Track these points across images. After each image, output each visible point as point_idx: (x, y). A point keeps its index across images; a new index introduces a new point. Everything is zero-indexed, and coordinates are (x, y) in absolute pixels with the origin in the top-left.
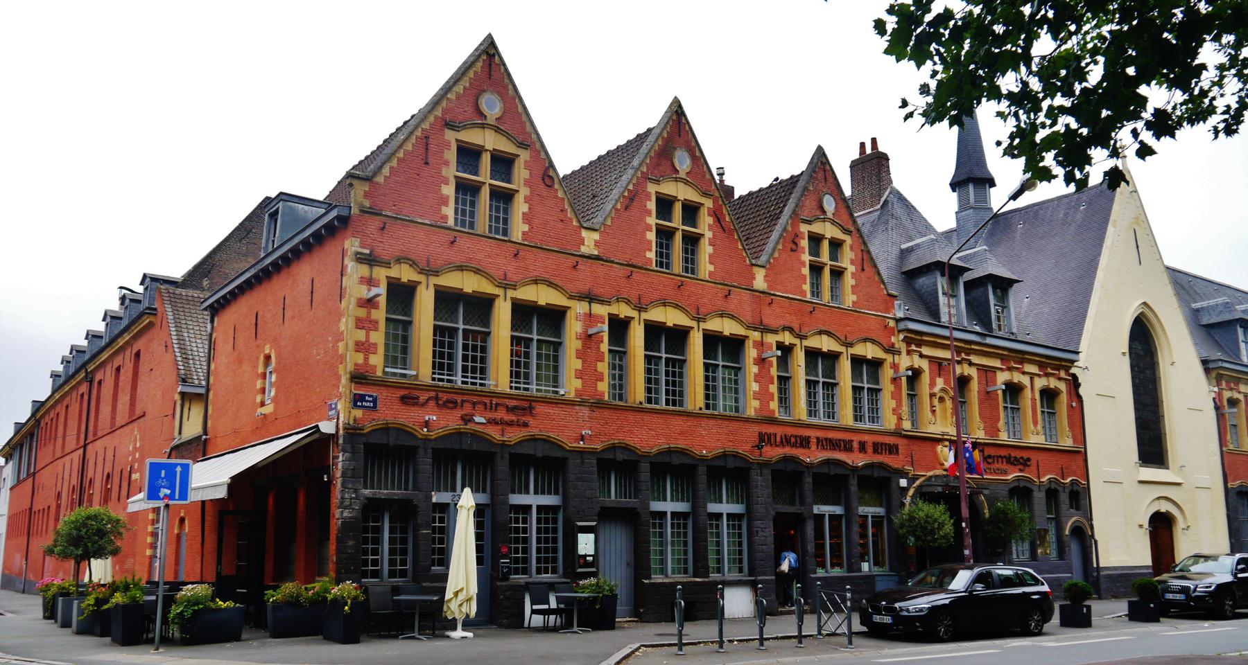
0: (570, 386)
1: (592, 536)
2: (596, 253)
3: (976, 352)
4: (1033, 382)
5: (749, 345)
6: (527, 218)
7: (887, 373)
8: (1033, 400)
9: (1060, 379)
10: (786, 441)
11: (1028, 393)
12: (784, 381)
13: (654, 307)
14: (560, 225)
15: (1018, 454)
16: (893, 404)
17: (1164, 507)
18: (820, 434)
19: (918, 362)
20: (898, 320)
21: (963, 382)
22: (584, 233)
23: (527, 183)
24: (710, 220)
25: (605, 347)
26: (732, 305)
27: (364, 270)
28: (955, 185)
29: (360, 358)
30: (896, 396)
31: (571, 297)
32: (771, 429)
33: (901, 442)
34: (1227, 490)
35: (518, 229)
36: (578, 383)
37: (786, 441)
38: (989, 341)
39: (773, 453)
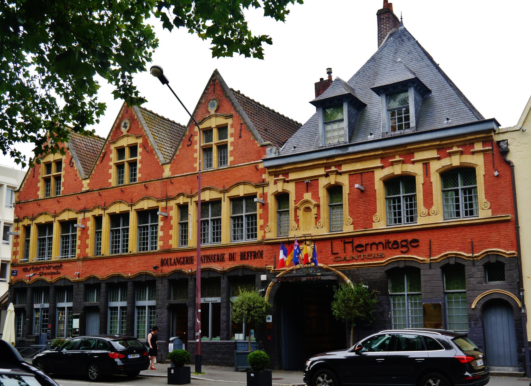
1: (78, 320)
2: (88, 189)
3: (345, 162)
10: (178, 261)
13: (153, 200)
14: (75, 182)
15: (399, 238)
18: (243, 250)
22: (84, 182)
26: (150, 192)
31: (77, 213)
32: (168, 256)
33: (265, 248)
37: (178, 261)
39: (168, 270)
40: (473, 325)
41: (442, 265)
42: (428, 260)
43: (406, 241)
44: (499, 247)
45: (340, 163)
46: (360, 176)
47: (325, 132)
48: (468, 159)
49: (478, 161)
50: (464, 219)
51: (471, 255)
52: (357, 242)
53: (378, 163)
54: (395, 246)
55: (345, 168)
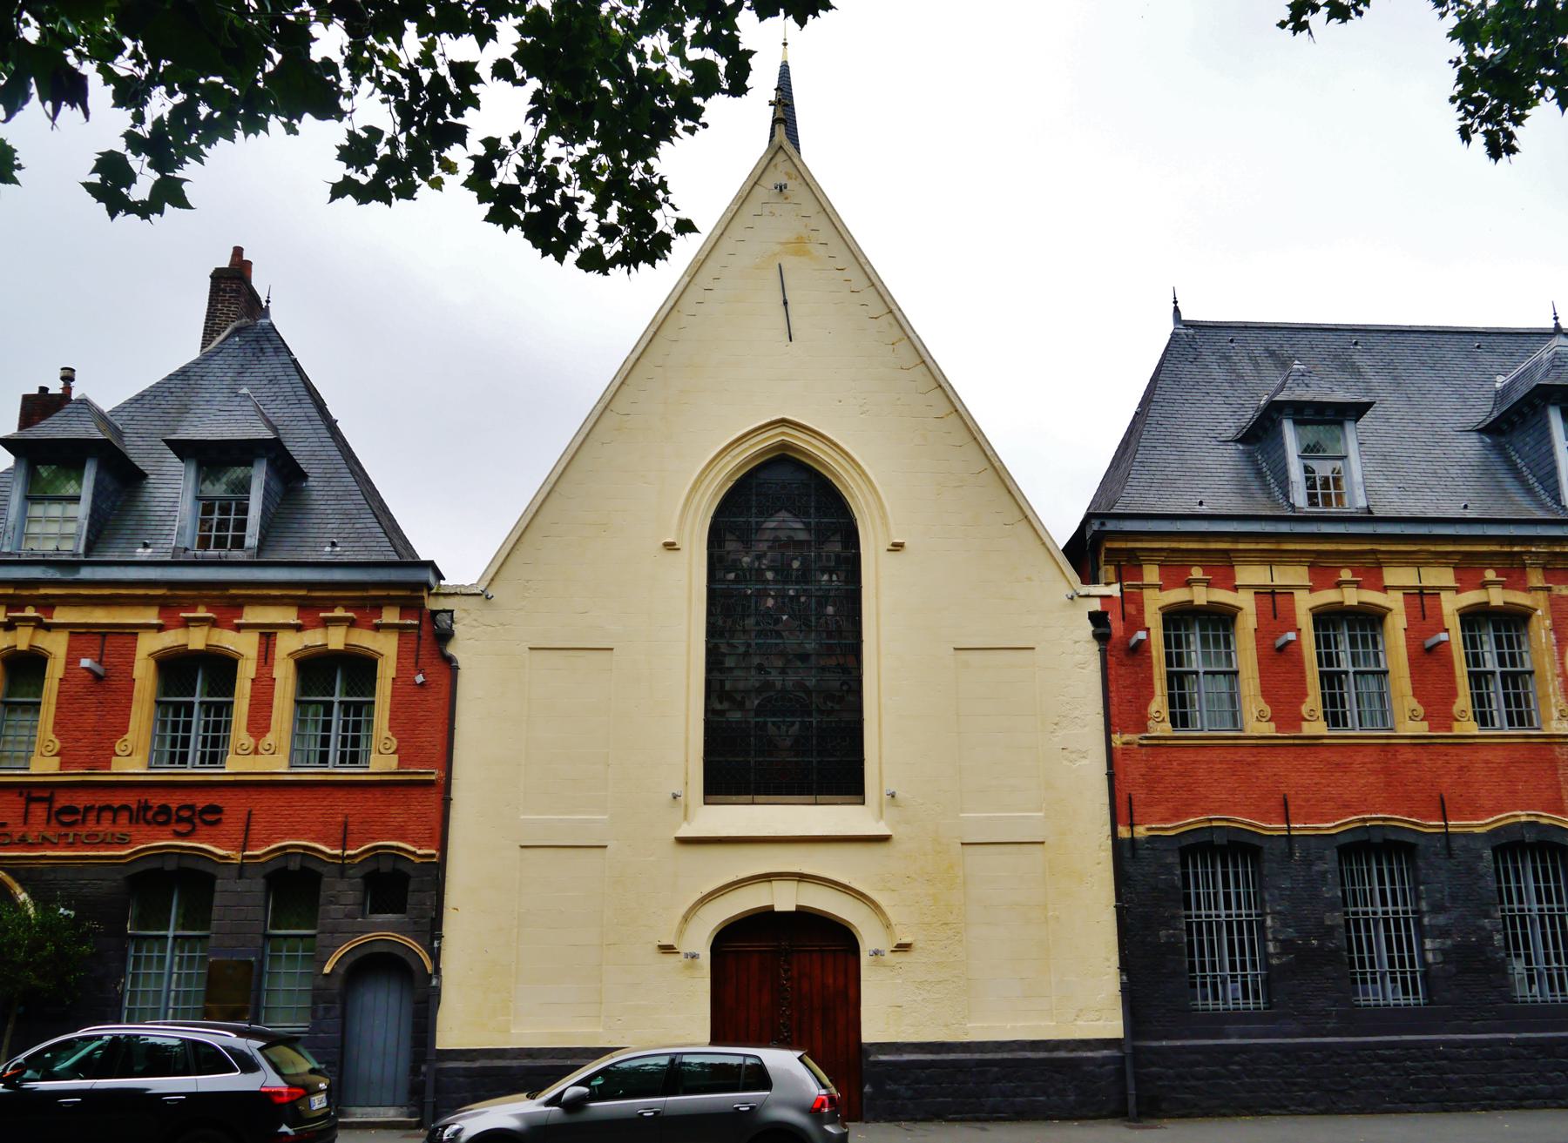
3: (66, 601)
15: (174, 801)
40: (320, 1014)
41: (269, 869)
42: (236, 857)
43: (191, 807)
44: (402, 838)
45: (51, 601)
46: (98, 641)
47: (25, 518)
48: (365, 640)
49: (386, 647)
50: (336, 770)
51: (338, 852)
52: (62, 800)
53: (151, 616)
54: (161, 819)
55: (61, 616)
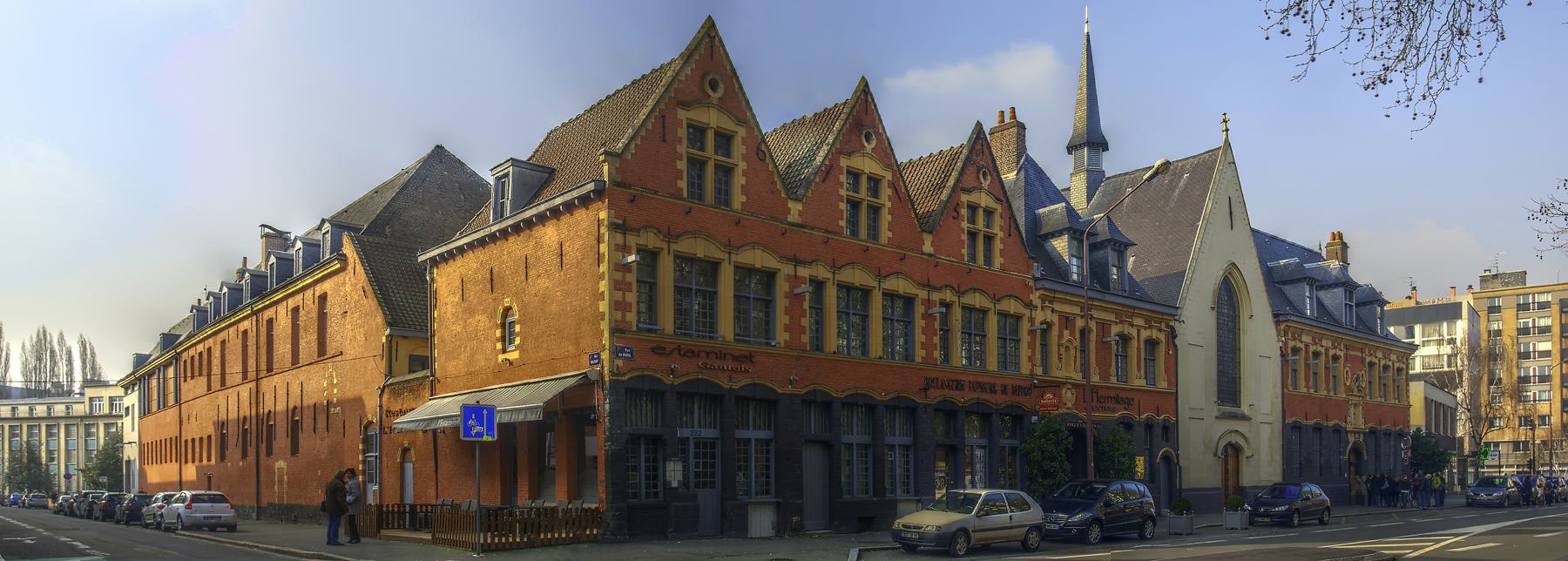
0: (782, 336)
4: (1139, 331)
5: (918, 303)
6: (745, 190)
7: (1025, 326)
8: (1139, 349)
9: (1160, 330)
11: (1134, 343)
12: (946, 333)
16: (1029, 352)
17: (1235, 439)
19: (1050, 317)
20: (1036, 280)
21: (1084, 333)
22: (791, 204)
23: (745, 158)
24: (890, 192)
25: (806, 305)
27: (619, 238)
28: (1071, 149)
29: (619, 315)
30: (1031, 346)
34: (1284, 425)
35: (738, 199)
36: (787, 336)
38: (1108, 298)
39: (936, 395)
52: (1102, 393)
